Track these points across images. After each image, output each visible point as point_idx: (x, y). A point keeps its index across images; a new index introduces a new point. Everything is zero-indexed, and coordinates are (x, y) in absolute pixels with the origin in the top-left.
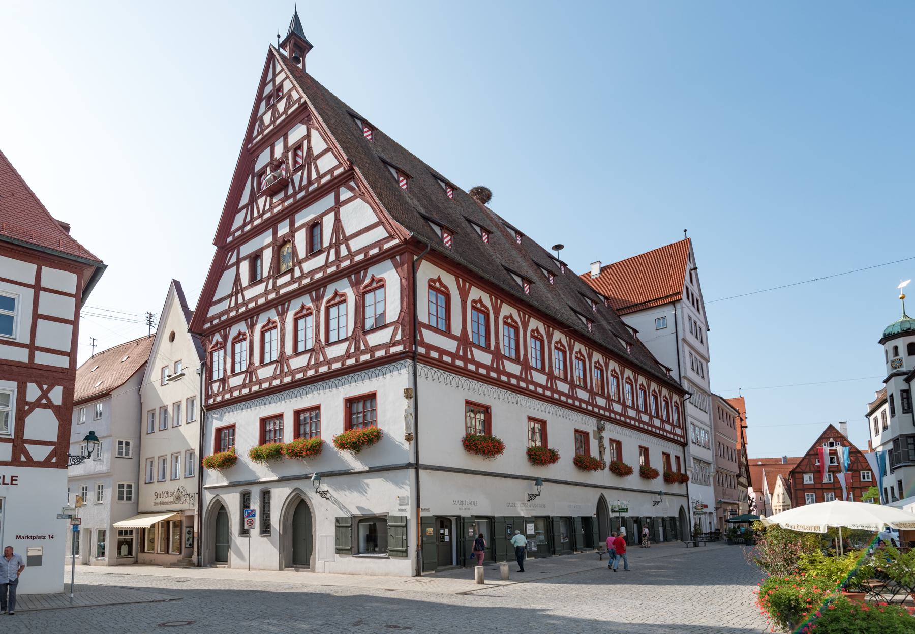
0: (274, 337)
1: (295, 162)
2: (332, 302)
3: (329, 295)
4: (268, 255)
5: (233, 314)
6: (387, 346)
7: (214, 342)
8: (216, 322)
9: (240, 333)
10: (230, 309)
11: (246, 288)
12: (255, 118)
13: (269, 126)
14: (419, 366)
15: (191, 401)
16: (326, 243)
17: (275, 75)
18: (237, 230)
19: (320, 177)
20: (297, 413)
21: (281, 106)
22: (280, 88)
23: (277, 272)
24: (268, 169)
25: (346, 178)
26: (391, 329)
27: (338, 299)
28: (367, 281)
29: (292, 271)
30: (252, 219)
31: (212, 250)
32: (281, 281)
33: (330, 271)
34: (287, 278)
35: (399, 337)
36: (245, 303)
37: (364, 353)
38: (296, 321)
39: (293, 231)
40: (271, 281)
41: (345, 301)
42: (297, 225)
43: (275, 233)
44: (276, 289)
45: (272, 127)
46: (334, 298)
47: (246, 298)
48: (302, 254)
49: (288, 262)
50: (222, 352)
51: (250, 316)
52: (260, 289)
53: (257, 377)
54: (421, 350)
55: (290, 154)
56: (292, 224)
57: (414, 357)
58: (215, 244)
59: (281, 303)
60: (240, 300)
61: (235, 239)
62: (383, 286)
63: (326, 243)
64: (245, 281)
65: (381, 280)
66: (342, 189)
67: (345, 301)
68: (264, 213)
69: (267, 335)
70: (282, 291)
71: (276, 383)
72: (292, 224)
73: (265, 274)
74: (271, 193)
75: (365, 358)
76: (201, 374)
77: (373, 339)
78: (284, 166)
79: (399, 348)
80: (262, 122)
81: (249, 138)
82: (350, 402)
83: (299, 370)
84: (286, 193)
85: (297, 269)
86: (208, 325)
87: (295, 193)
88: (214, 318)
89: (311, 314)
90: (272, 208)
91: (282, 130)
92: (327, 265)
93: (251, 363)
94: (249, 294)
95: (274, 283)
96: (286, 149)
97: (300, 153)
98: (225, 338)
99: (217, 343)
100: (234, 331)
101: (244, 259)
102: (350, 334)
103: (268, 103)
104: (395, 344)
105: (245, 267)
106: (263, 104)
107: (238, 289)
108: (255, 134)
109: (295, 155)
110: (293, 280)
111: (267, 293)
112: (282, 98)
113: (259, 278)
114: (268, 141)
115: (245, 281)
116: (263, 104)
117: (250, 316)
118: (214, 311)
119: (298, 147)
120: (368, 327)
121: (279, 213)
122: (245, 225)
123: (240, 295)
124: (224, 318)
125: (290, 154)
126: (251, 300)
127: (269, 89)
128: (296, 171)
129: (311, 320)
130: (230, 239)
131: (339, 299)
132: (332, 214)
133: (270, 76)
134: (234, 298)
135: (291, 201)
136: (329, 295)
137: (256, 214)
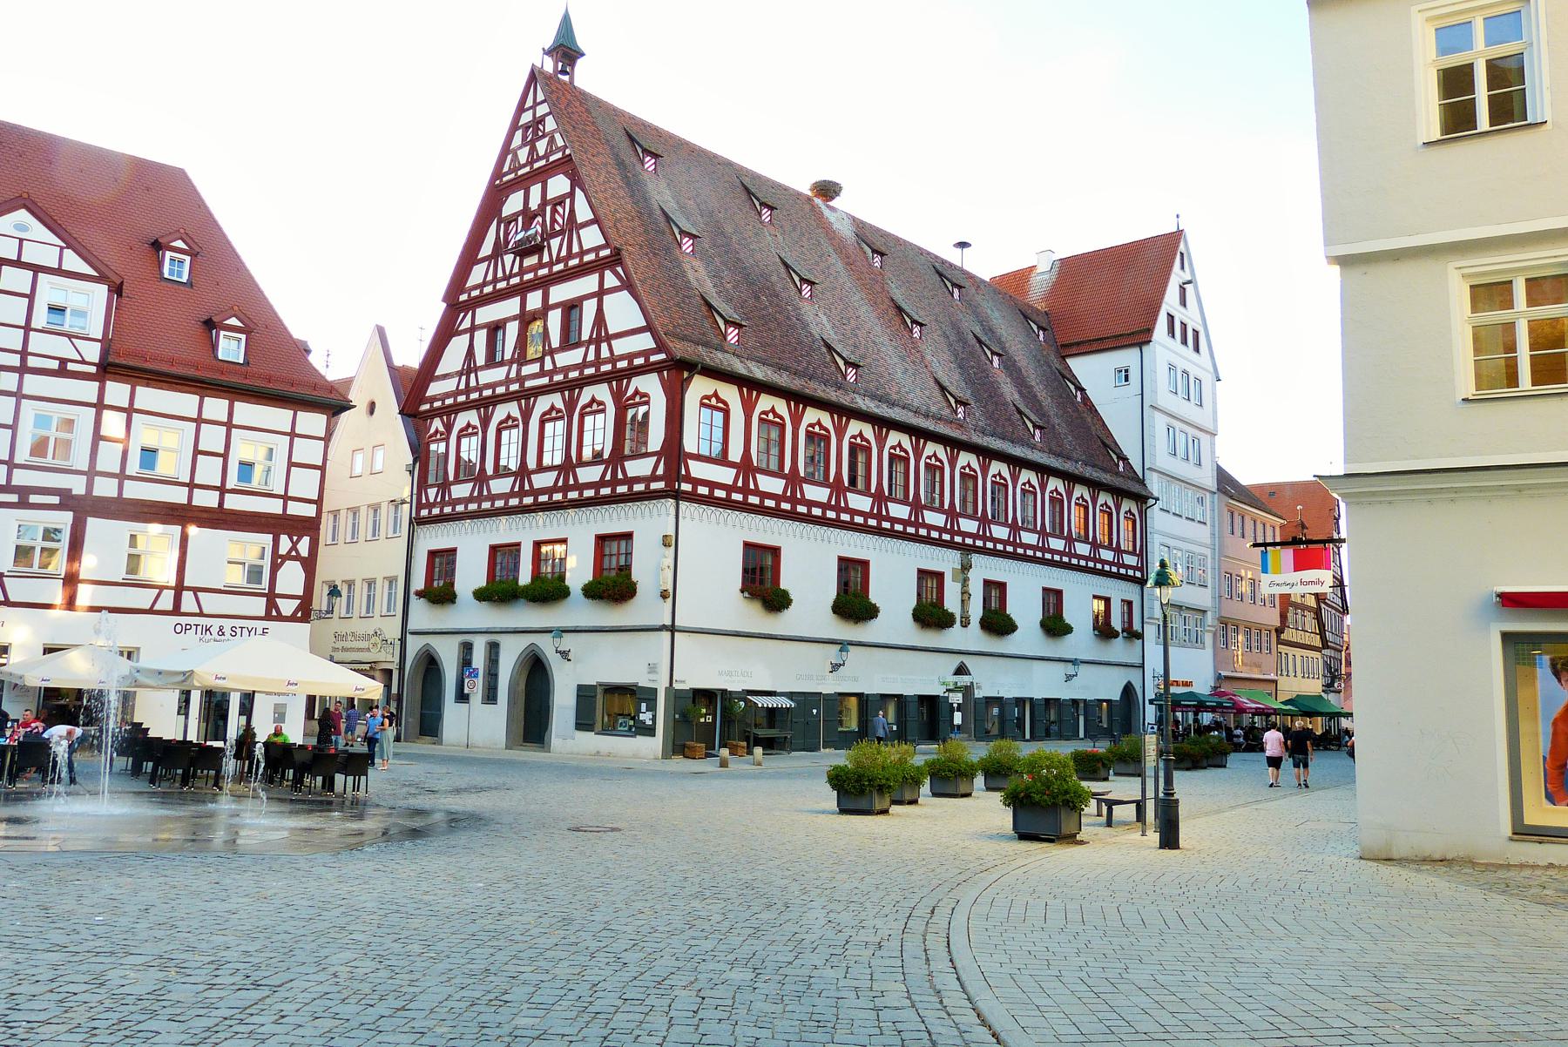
0: (514, 439)
1: (553, 221)
3: (584, 399)
5: (462, 398)
7: (432, 430)
8: (437, 404)
9: (469, 425)
10: (458, 392)
11: (482, 368)
12: (506, 149)
13: (524, 166)
14: (683, 505)
15: (396, 504)
16: (585, 336)
17: (536, 104)
18: (475, 287)
19: (583, 253)
20: (538, 545)
21: (541, 146)
22: (542, 120)
23: (521, 358)
25: (615, 260)
27: (595, 407)
28: (630, 392)
29: (541, 360)
30: (495, 280)
34: (535, 368)
36: (479, 389)
37: (622, 483)
38: (542, 423)
39: (547, 307)
40: (515, 366)
41: (603, 411)
42: (551, 302)
44: (520, 379)
45: (527, 169)
46: (590, 405)
47: (481, 382)
48: (555, 343)
51: (485, 405)
52: (498, 374)
53: (489, 490)
54: (686, 487)
55: (548, 209)
56: (546, 297)
57: (678, 496)
60: (473, 383)
61: (470, 299)
62: (647, 403)
63: (585, 336)
64: (480, 359)
65: (646, 395)
67: (603, 411)
68: (512, 276)
69: (505, 434)
70: (528, 384)
71: (514, 502)
72: (546, 297)
73: (508, 356)
74: (523, 251)
75: (622, 489)
76: (411, 473)
78: (539, 219)
81: (498, 173)
82: (602, 539)
83: (543, 491)
84: (541, 259)
85: (548, 359)
86: (427, 407)
87: (551, 264)
88: (433, 399)
89: (561, 418)
90: (522, 271)
91: (542, 176)
93: (482, 469)
95: (519, 371)
96: (544, 202)
97: (560, 209)
98: (449, 427)
100: (461, 420)
101: (482, 327)
103: (524, 137)
105: (481, 337)
106: (519, 134)
107: (470, 368)
108: (506, 169)
109: (554, 211)
111: (507, 381)
112: (544, 136)
113: (498, 358)
114: (523, 183)
115: (480, 359)
116: (519, 134)
117: (485, 405)
118: (435, 389)
119: (559, 201)
120: (627, 452)
121: (530, 281)
122: (485, 284)
124: (449, 401)
125: (548, 209)
126: (487, 386)
128: (554, 235)
129: (560, 425)
130: (464, 297)
131: (596, 407)
133: (529, 103)
135: (544, 271)
136: (584, 399)
137: (500, 274)
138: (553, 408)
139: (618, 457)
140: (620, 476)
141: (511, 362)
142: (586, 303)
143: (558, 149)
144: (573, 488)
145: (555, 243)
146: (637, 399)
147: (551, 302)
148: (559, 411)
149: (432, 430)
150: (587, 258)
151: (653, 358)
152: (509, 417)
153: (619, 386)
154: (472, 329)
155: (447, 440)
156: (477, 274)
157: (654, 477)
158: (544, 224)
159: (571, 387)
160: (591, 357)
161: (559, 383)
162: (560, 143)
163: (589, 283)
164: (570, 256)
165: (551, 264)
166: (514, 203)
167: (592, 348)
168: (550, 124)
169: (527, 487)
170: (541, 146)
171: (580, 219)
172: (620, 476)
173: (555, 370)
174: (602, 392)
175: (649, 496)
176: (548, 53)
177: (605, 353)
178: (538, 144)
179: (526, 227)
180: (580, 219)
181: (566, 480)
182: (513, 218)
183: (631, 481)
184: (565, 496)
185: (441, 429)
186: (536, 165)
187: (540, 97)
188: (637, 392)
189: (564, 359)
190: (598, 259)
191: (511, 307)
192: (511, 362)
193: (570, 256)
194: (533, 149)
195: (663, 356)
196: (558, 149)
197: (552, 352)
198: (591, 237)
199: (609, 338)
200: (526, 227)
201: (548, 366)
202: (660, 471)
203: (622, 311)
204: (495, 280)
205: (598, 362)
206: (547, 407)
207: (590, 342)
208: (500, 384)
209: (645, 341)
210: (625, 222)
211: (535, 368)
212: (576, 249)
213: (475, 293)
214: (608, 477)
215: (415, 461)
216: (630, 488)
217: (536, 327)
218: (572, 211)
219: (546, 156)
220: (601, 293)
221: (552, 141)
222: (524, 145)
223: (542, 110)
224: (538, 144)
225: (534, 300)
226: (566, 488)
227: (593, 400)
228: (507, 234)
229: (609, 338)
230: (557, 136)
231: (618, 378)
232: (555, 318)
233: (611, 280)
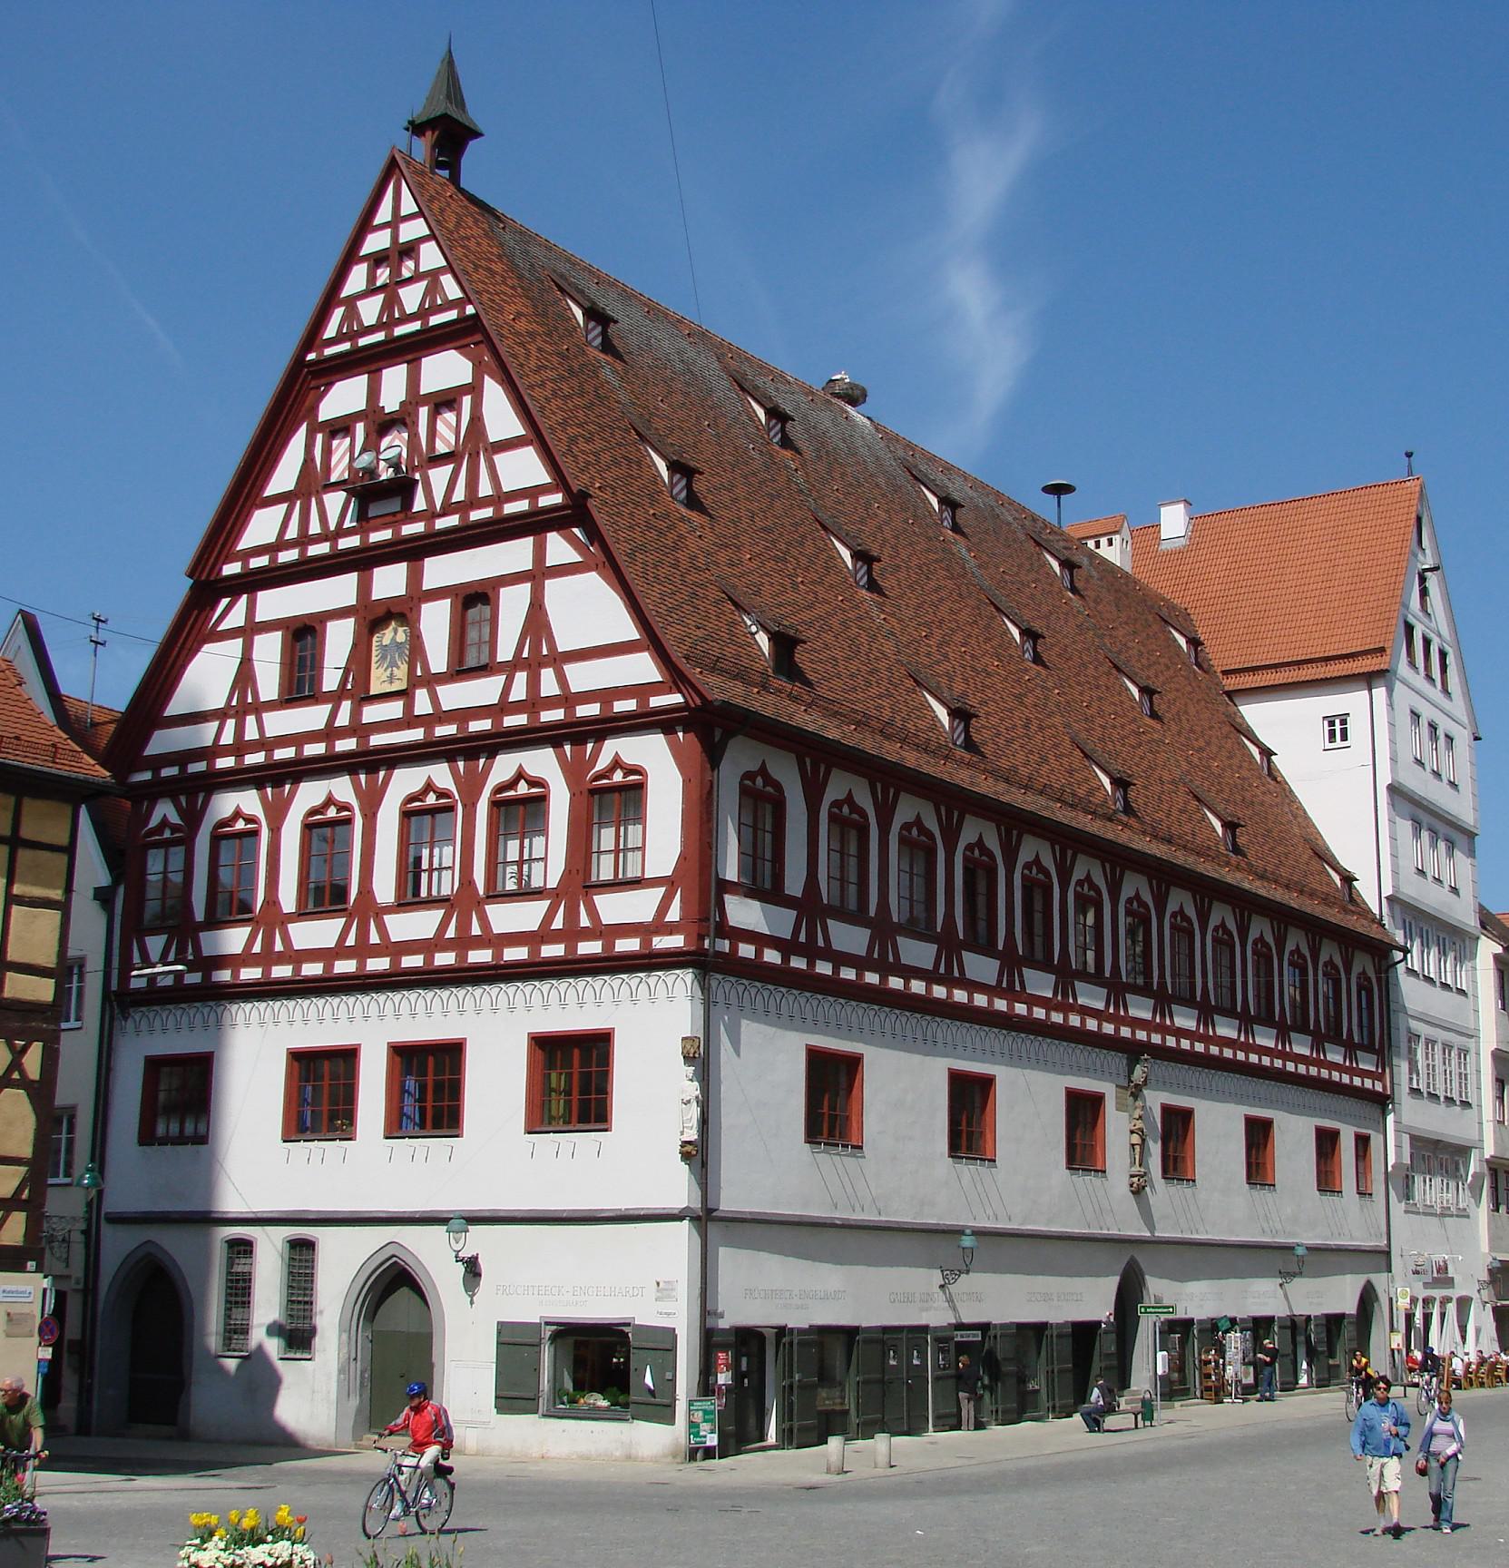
4: (339, 640)
8: (168, 772)
11: (272, 706)
12: (331, 298)
16: (505, 653)
18: (258, 551)
21: (411, 297)
22: (410, 250)
24: (360, 428)
25: (574, 514)
26: (660, 892)
28: (603, 763)
29: (406, 695)
31: (183, 587)
32: (371, 714)
33: (511, 721)
34: (394, 710)
36: (265, 744)
37: (587, 934)
39: (417, 596)
40: (346, 705)
41: (542, 799)
42: (428, 584)
43: (365, 588)
44: (359, 729)
45: (380, 336)
46: (512, 784)
48: (438, 660)
49: (393, 664)
50: (178, 854)
52: (312, 717)
53: (286, 939)
55: (424, 412)
56: (415, 578)
58: (190, 576)
59: (372, 763)
60: (251, 733)
62: (640, 787)
63: (505, 653)
66: (555, 541)
68: (341, 532)
70: (377, 740)
72: (415, 578)
77: (613, 908)
80: (352, 314)
81: (312, 337)
93: (272, 900)
94: (281, 723)
95: (356, 713)
96: (414, 398)
98: (193, 817)
99: (165, 823)
102: (553, 883)
103: (372, 277)
104: (671, 929)
105: (269, 649)
108: (330, 331)
110: (409, 721)
111: (330, 733)
114: (368, 362)
115: (269, 687)
119: (445, 401)
122: (281, 544)
123: (251, 720)
125: (424, 412)
126: (283, 741)
127: (376, 242)
132: (525, 589)
133: (384, 214)
134: (231, 723)
137: (315, 528)
138: (429, 787)
139: (580, 883)
140: (585, 922)
141: (336, 698)
142: (505, 593)
143: (449, 305)
144: (479, 943)
145: (439, 477)
146: (618, 777)
147: (428, 584)
148: (442, 794)
149: (155, 821)
150: (510, 508)
152: (330, 801)
154: (251, 630)
155: (188, 842)
156: (262, 527)
157: (660, 925)
158: (413, 442)
159: (471, 750)
160: (519, 692)
162: (452, 290)
163: (515, 554)
164: (473, 501)
165: (430, 515)
166: (345, 397)
167: (521, 678)
168: (431, 256)
169: (374, 938)
170: (411, 297)
171: (494, 435)
172: (585, 922)
173: (440, 716)
174: (543, 763)
176: (417, 129)
177: (549, 686)
178: (403, 292)
179: (371, 445)
180: (494, 435)
181: (464, 926)
182: (340, 427)
183: (612, 932)
184: (462, 956)
185: (174, 818)
186: (400, 331)
187: (408, 206)
188: (617, 763)
189: (455, 696)
190: (535, 512)
191: (340, 590)
192: (336, 698)
193: (473, 501)
194: (392, 301)
195: (677, 699)
196: (449, 305)
197: (431, 681)
198: (523, 469)
199: (559, 660)
200: (371, 445)
201: (422, 704)
202: (674, 914)
203: (588, 610)
204: (304, 540)
205: (534, 703)
206: (417, 786)
208: (312, 737)
209: (643, 668)
210: (582, 444)
211: (394, 710)
212: (485, 489)
213: (256, 563)
214: (558, 923)
215: (116, 881)
216: (609, 945)
217: (393, 634)
218: (477, 418)
219: (422, 314)
220: (538, 575)
221: (434, 287)
222: (371, 291)
223: (413, 230)
224: (403, 292)
225: (390, 581)
226: (463, 943)
227: (520, 775)
228: (328, 452)
229: (559, 660)
230: (447, 281)
231: (575, 735)
232: (436, 621)
233: (559, 549)
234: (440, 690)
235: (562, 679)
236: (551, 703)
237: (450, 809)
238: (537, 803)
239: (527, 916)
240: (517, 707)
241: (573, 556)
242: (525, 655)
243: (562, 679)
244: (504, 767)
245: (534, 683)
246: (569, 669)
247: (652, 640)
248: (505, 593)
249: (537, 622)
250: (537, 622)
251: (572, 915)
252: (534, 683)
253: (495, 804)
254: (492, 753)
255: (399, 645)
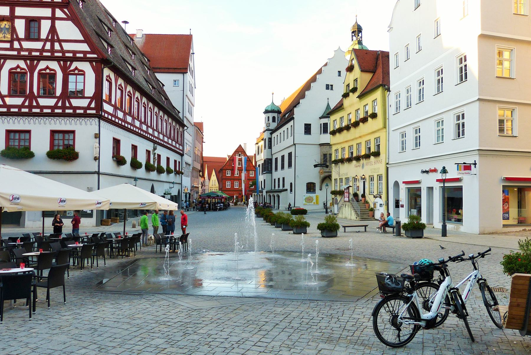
2: (44, 72)
6: (85, 109)
16: (43, 36)
28: (72, 68)
29: (11, 42)
34: (8, 45)
35: (93, 105)
46: (45, 69)
48: (21, 34)
62: (84, 74)
79: (94, 112)
92: (43, 50)
102: (58, 93)
110: (12, 48)
146: (76, 72)
151: (88, 56)
153: (65, 64)
161: (24, 56)
172: (67, 105)
174: (54, 65)
175: (85, 115)
188: (76, 68)
199: (60, 41)
206: (14, 66)
207: (46, 40)
211: (8, 45)
220: (53, 19)
227: (47, 67)
231: (65, 60)
233: (59, 13)
234: (22, 43)
235: (61, 46)
236: (58, 51)
237: (26, 73)
238: (53, 76)
239: (51, 102)
240: (47, 51)
241: (64, 16)
242: (50, 38)
243: (61, 46)
244: (42, 65)
245: (52, 46)
246: (63, 44)
247: (86, 40)
248: (43, 22)
249: (53, 30)
250: (53, 30)
251: (64, 103)
252: (52, 46)
253: (39, 74)
254: (39, 61)
255: (7, 29)
